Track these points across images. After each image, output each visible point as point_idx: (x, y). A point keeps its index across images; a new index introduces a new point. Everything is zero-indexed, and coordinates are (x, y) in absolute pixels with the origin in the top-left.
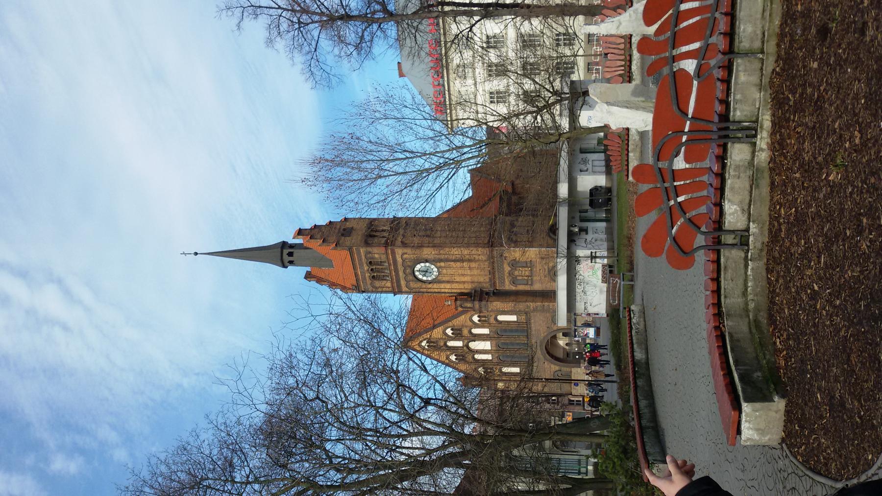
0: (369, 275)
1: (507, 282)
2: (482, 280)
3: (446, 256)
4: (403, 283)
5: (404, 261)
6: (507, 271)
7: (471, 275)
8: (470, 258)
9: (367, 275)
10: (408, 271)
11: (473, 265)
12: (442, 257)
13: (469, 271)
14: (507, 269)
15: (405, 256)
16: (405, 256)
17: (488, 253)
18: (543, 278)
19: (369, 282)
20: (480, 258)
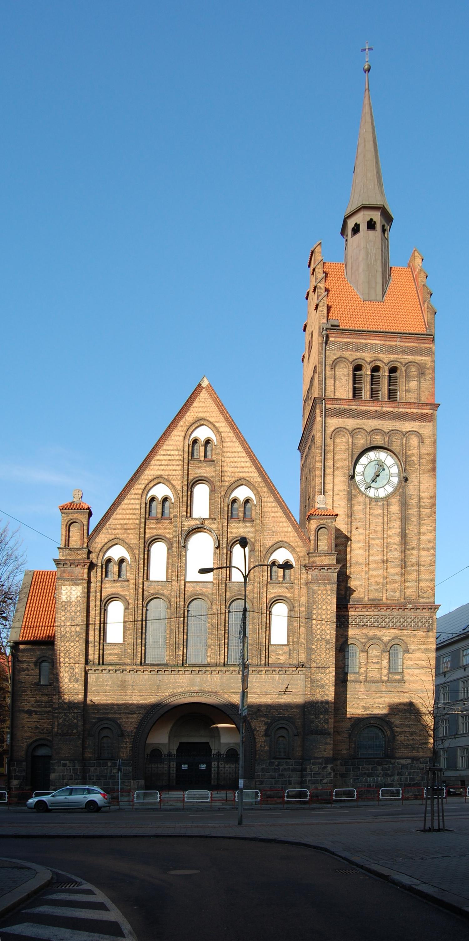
0: (368, 360)
3: (414, 519)
5: (406, 434)
8: (409, 564)
9: (367, 356)
11: (394, 570)
12: (413, 511)
13: (379, 559)
14: (387, 635)
15: (414, 441)
16: (414, 441)
17: (422, 600)
18: (362, 703)
20: (408, 584)
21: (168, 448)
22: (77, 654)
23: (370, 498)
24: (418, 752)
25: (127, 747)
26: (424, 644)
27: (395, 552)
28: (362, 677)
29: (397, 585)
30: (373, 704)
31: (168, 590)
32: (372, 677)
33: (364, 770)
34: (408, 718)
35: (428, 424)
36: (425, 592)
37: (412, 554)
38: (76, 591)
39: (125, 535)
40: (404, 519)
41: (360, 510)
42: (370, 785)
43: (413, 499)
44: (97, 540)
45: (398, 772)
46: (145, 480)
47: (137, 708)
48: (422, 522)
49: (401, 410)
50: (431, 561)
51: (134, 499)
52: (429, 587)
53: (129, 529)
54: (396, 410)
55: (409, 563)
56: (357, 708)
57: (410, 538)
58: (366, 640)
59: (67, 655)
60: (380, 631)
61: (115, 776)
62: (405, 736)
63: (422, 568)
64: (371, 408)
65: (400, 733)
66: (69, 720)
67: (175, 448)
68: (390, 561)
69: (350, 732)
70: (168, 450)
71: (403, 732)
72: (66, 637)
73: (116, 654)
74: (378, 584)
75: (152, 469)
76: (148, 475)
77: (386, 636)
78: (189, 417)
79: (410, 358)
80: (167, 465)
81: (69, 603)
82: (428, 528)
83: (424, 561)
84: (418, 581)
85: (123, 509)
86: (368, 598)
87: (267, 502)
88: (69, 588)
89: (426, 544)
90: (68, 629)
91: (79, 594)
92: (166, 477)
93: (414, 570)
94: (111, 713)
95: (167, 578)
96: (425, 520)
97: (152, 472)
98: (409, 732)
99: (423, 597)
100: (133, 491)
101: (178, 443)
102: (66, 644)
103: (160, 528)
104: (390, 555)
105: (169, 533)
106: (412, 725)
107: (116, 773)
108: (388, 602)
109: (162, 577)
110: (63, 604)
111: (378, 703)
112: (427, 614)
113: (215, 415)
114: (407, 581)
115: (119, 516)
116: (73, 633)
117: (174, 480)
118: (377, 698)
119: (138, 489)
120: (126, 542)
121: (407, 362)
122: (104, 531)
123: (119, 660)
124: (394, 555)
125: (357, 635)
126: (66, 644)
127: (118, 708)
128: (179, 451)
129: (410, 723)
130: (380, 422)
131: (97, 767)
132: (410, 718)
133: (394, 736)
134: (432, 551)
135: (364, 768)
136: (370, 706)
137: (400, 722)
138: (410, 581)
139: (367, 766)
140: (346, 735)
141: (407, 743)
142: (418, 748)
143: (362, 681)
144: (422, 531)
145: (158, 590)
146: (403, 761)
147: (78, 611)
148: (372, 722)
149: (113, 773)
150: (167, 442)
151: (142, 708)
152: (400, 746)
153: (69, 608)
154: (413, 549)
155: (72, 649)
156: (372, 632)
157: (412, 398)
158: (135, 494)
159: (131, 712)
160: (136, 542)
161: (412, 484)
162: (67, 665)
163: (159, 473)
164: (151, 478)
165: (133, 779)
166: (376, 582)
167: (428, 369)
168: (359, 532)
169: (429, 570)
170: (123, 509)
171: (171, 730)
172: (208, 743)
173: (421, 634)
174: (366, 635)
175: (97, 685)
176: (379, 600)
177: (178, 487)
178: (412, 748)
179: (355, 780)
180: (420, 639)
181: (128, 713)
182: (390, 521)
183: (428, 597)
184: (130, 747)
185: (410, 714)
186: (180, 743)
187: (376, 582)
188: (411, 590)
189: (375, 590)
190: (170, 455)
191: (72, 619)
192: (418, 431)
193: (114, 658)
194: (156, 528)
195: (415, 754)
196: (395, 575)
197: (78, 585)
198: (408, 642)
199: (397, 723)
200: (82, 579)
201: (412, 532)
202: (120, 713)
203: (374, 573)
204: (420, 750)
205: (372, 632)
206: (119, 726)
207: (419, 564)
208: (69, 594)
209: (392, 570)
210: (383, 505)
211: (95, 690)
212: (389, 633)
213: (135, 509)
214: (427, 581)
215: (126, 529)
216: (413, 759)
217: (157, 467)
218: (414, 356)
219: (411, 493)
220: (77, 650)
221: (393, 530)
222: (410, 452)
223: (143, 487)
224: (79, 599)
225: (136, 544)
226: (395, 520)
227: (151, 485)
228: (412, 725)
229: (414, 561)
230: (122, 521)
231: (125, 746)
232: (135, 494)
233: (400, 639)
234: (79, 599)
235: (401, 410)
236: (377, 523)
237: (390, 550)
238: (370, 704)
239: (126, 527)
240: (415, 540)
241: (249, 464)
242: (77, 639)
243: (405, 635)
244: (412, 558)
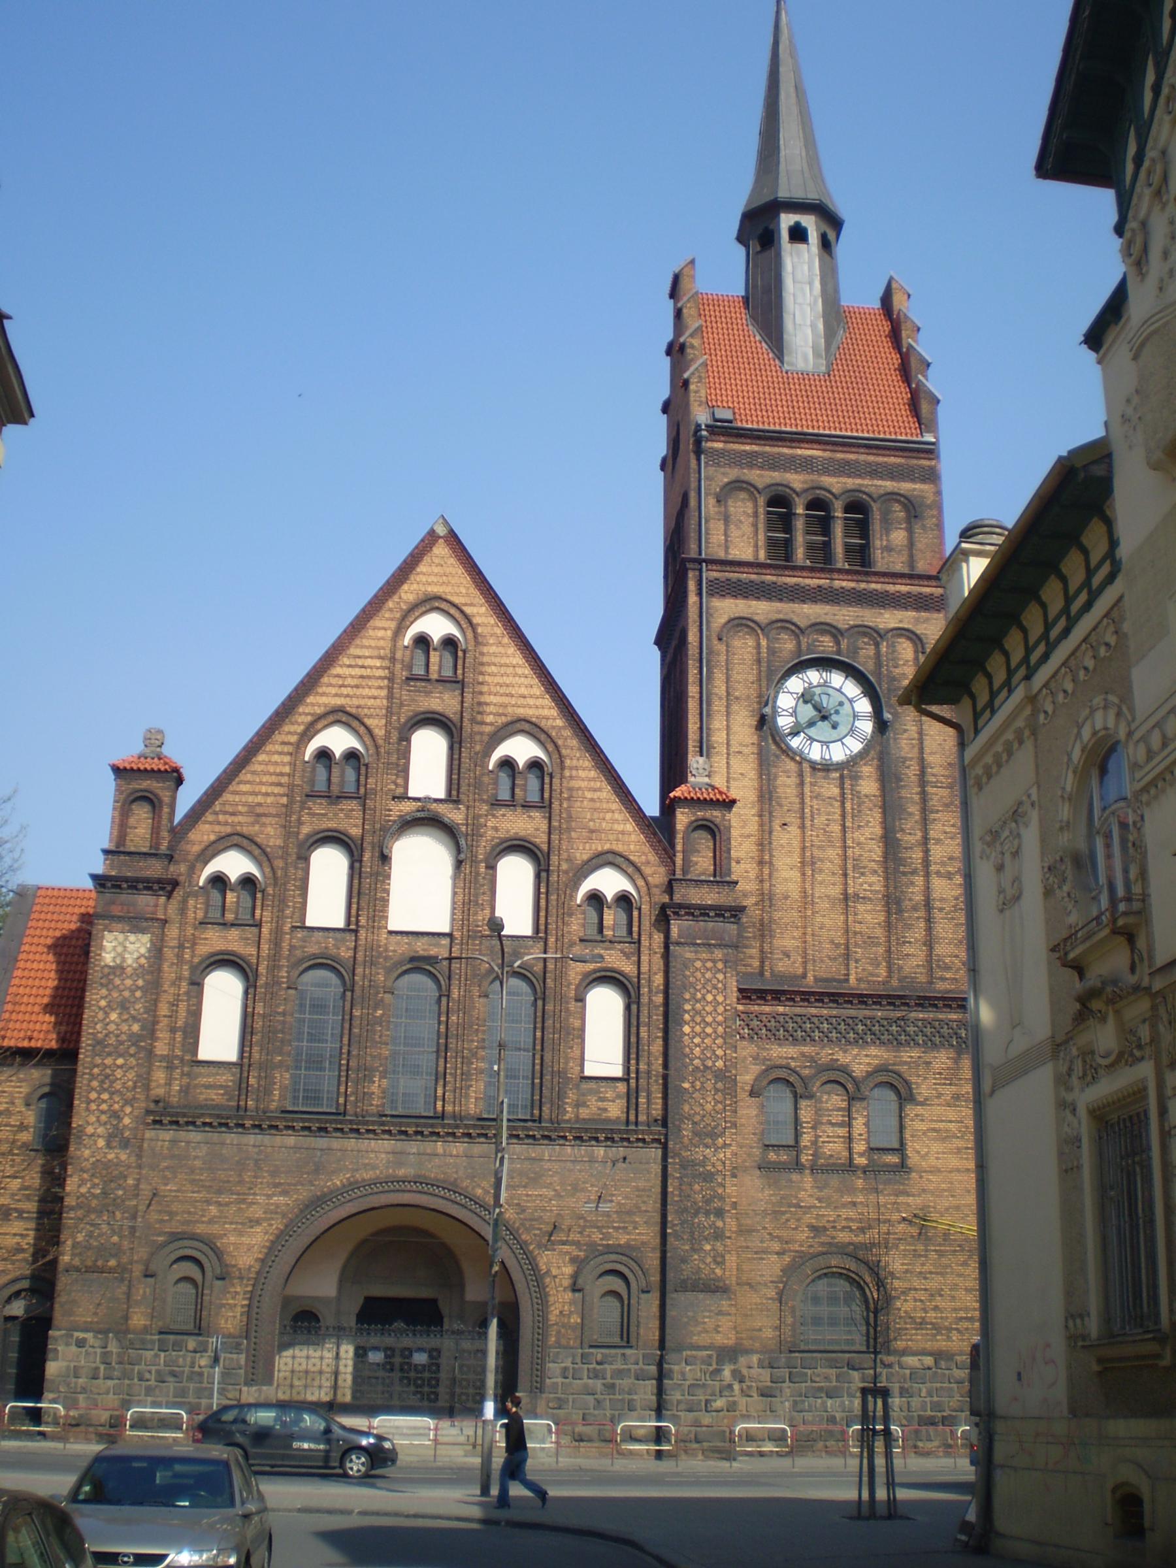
2: (787, 940)
4: (762, 609)
6: (843, 1058)
7: (807, 900)
11: (870, 917)
12: (911, 792)
17: (941, 986)
18: (808, 1219)
19: (761, 477)
21: (358, 652)
22: (130, 1083)
23: (814, 765)
24: (949, 1339)
25: (235, 1305)
26: (950, 1084)
27: (874, 879)
28: (807, 1155)
29: (881, 950)
30: (834, 1221)
31: (348, 949)
32: (831, 1156)
33: (817, 1379)
35: (935, 615)
36: (947, 968)
37: (912, 883)
38: (137, 945)
39: (257, 828)
40: (890, 808)
41: (789, 786)
42: (834, 1417)
43: (908, 767)
44: (193, 836)
45: (901, 1388)
46: (307, 714)
47: (265, 1213)
48: (933, 816)
49: (873, 586)
50: (956, 899)
51: (281, 753)
52: (956, 956)
53: (265, 815)
54: (863, 585)
55: (907, 902)
56: (796, 1229)
57: (906, 848)
58: (813, 1071)
59: (105, 1086)
60: (845, 1052)
61: (201, 1374)
62: (915, 1300)
64: (808, 581)
65: (903, 1293)
66: (100, 1235)
67: (375, 653)
68: (863, 898)
69: (781, 1285)
70: (359, 657)
71: (910, 1289)
72: (106, 1046)
73: (221, 1087)
74: (837, 946)
75: (323, 694)
76: (313, 705)
77: (860, 1064)
78: (409, 592)
79: (889, 485)
80: (357, 687)
81: (119, 970)
82: (948, 829)
83: (942, 900)
84: (929, 942)
85: (254, 773)
86: (815, 976)
87: (576, 768)
88: (121, 937)
89: (943, 864)
90: (112, 1027)
91: (143, 950)
92: (353, 711)
93: (918, 918)
94: (203, 1222)
95: (348, 922)
96: (937, 812)
97: (324, 700)
98: (926, 1290)
99: (943, 979)
100: (277, 737)
101: (382, 643)
102: (106, 1061)
103: (336, 815)
104: (861, 885)
105: (355, 826)
106: (931, 1273)
107: (206, 1366)
108: (862, 986)
109: (337, 920)
110: (106, 970)
111: (846, 1219)
112: (954, 1016)
113: (464, 591)
114: (904, 942)
115: (245, 788)
116: (124, 1037)
117: (370, 717)
118: (844, 1206)
119: (289, 733)
120: (256, 844)
121: (882, 492)
122: (209, 817)
123: (228, 1100)
124: (870, 885)
125: (792, 1058)
126: (106, 1061)
127: (221, 1212)
128: (380, 657)
130: (828, 608)
131: (160, 1350)
132: (926, 1256)
133: (889, 1300)
135: (819, 1375)
136: (828, 1225)
138: (910, 942)
139: (824, 1370)
140: (772, 1293)
142: (949, 1329)
143: (807, 1164)
144: (932, 834)
145: (326, 948)
146: (911, 1361)
147: (138, 988)
148: (833, 1263)
149: (200, 1367)
150: (358, 641)
151: (276, 1213)
152: (906, 1323)
153: (117, 981)
154: (914, 872)
155: (119, 1073)
156: (827, 1054)
157: (899, 564)
158: (284, 743)
159: (251, 1221)
160: (279, 842)
161: (905, 735)
162: (104, 1107)
163: (339, 701)
164: (319, 711)
165: (246, 1384)
166: (832, 942)
167: (930, 507)
168: (789, 832)
169: (953, 918)
170: (254, 773)
171: (344, 1268)
172: (434, 1302)
174: (812, 1059)
175: (173, 1157)
176: (839, 981)
177: (380, 732)
179: (795, 1402)
180: (940, 1074)
181: (242, 1224)
182: (859, 811)
184: (243, 1306)
185: (926, 1245)
186: (368, 1300)
187: (832, 942)
188: (914, 962)
189: (830, 959)
190: (363, 667)
191: (124, 1006)
192: (914, 629)
193: (217, 1094)
194: (325, 815)
195: (941, 1343)
196: (874, 928)
197: (143, 931)
198: (913, 1079)
200: (152, 919)
201: (910, 836)
202: (225, 1223)
203: (827, 922)
204: (955, 1336)
205: (827, 1054)
206: (218, 1253)
207: (928, 904)
208: (120, 949)
209: (869, 917)
210: (842, 777)
211: (167, 1168)
212: (867, 1056)
213: (282, 774)
214: (950, 944)
215: (259, 815)
216: (938, 1355)
217: (333, 691)
218: (898, 481)
219: (903, 754)
220: (131, 1075)
221: (867, 832)
222: (897, 671)
223: (300, 729)
224: (143, 961)
225: (280, 847)
226: (871, 810)
227: (319, 726)
228: (931, 1273)
229: (919, 898)
230: (250, 799)
231: (231, 1302)
232: (284, 743)
233: (891, 1071)
234: (143, 961)
235: (873, 586)
236: (827, 817)
237: (863, 874)
238: (828, 1221)
239: (259, 810)
240: (917, 855)
241: (538, 689)
242: (132, 1050)
243: (906, 1063)
244: (912, 893)
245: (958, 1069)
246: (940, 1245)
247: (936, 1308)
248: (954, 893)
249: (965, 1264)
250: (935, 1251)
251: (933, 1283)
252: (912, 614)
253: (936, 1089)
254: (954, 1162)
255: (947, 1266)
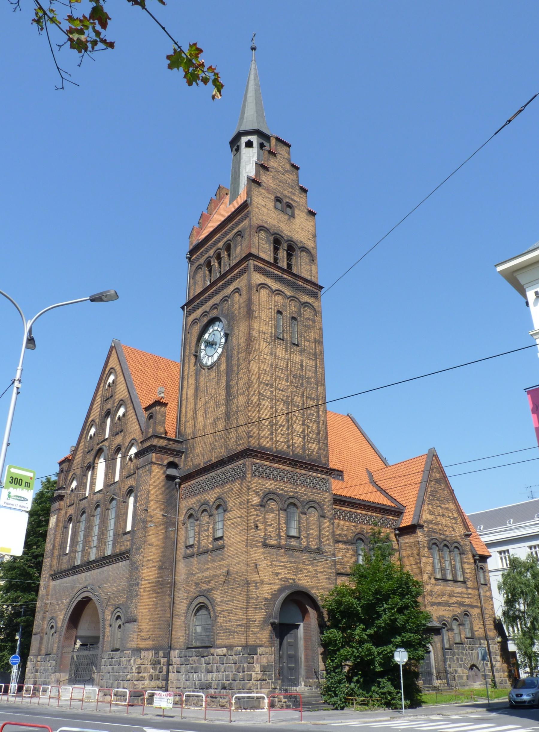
1: (192, 502)
10: (215, 313)
34: (226, 592)
36: (241, 439)
50: (245, 403)
60: (208, 494)
63: (240, 413)
82: (244, 371)
89: (242, 388)
98: (227, 610)
106: (229, 601)
129: (229, 598)
134: (246, 393)
137: (221, 597)
141: (225, 626)
144: (240, 376)
173: (236, 485)
178: (229, 632)
183: (244, 443)
198: (228, 499)
199: (218, 600)
228: (229, 601)
245: (242, 488)
246: (233, 585)
247: (230, 621)
248: (245, 400)
249: (240, 594)
250: (231, 588)
251: (229, 607)
252: (238, 280)
253: (234, 502)
254: (239, 538)
255: (234, 596)
